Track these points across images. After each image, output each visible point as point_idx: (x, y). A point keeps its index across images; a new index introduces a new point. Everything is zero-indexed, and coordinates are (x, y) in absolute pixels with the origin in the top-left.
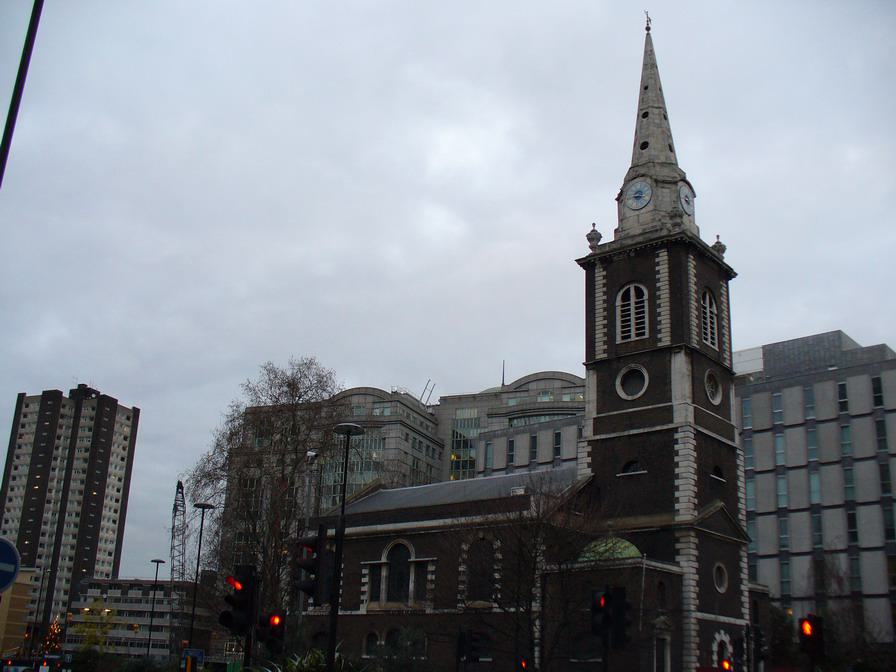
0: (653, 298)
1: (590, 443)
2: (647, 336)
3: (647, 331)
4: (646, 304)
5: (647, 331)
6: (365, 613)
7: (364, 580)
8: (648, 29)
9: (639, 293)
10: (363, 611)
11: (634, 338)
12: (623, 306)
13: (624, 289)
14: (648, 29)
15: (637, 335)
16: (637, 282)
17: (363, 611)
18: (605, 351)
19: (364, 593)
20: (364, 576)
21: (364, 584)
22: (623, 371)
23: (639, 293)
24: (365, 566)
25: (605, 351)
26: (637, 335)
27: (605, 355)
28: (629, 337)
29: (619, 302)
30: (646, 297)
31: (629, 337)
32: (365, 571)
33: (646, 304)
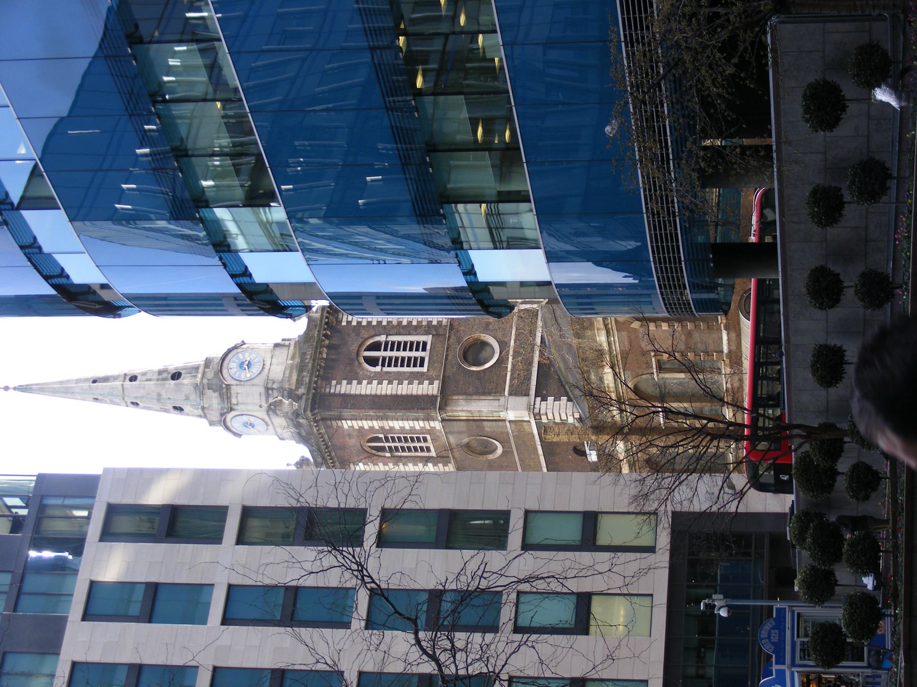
0: (388, 329)
2: (428, 339)
4: (392, 338)
5: (422, 338)
8: (6, 388)
9: (376, 347)
12: (383, 365)
13: (362, 360)
14: (6, 388)
15: (424, 349)
16: (362, 344)
18: (431, 383)
23: (376, 347)
25: (431, 383)
27: (436, 383)
28: (423, 359)
29: (378, 369)
30: (382, 338)
33: (392, 338)
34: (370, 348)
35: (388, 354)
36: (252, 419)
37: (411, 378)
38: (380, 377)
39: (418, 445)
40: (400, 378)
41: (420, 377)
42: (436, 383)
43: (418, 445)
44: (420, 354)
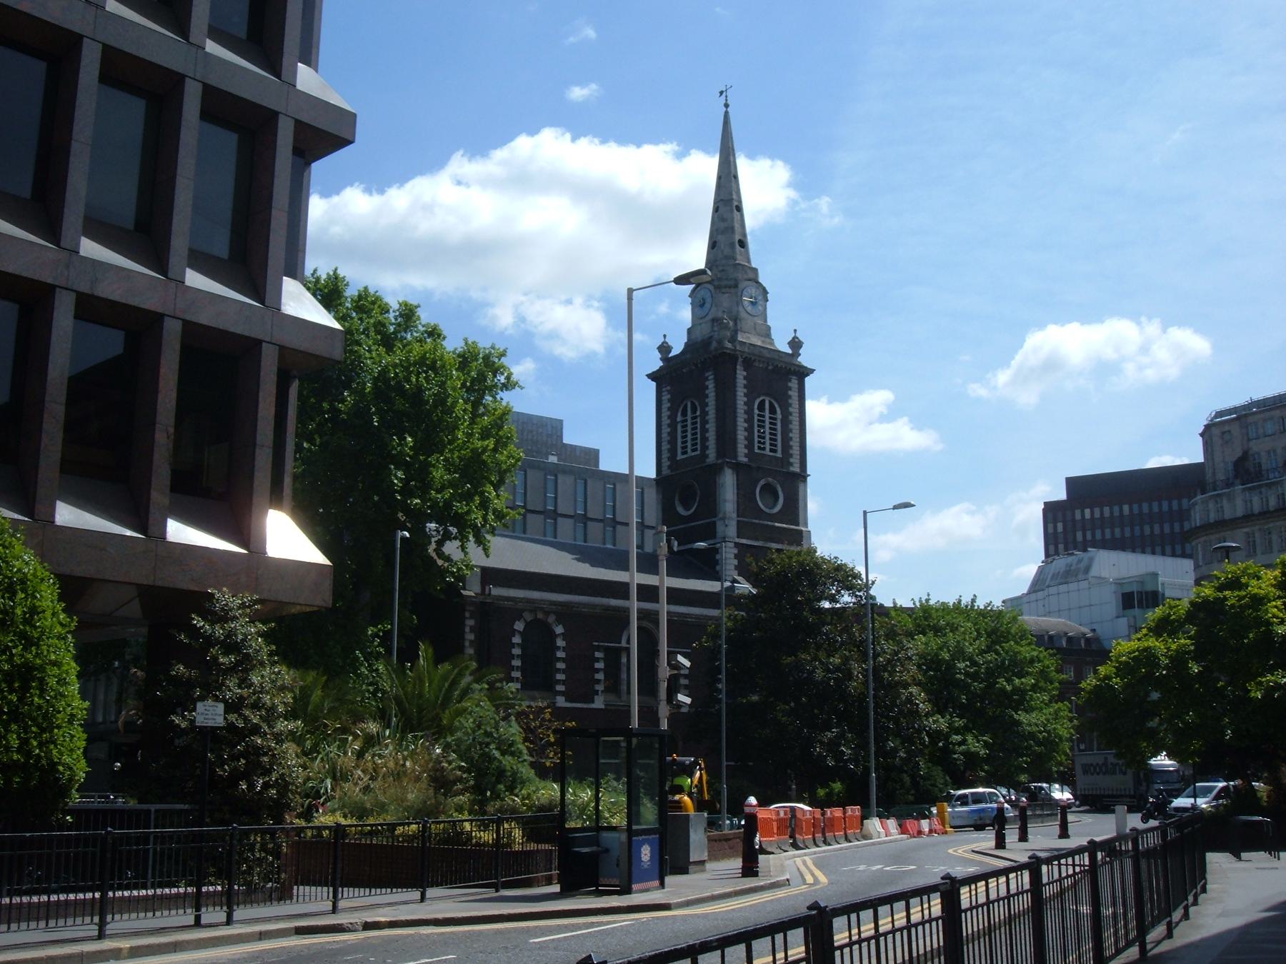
1: (737, 545)
2: (779, 455)
3: (779, 448)
5: (779, 448)
6: (603, 707)
7: (597, 665)
9: (773, 411)
10: (599, 703)
11: (767, 452)
15: (771, 450)
17: (599, 703)
19: (598, 681)
20: (598, 660)
21: (598, 671)
22: (762, 482)
23: (773, 411)
24: (598, 648)
26: (771, 450)
27: (746, 460)
29: (756, 411)
30: (779, 416)
31: (764, 449)
32: (598, 655)
34: (771, 405)
35: (767, 420)
36: (708, 305)
37: (750, 439)
38: (749, 412)
39: (689, 444)
40: (749, 430)
41: (750, 446)
42: (746, 460)
43: (689, 444)
44: (768, 447)
